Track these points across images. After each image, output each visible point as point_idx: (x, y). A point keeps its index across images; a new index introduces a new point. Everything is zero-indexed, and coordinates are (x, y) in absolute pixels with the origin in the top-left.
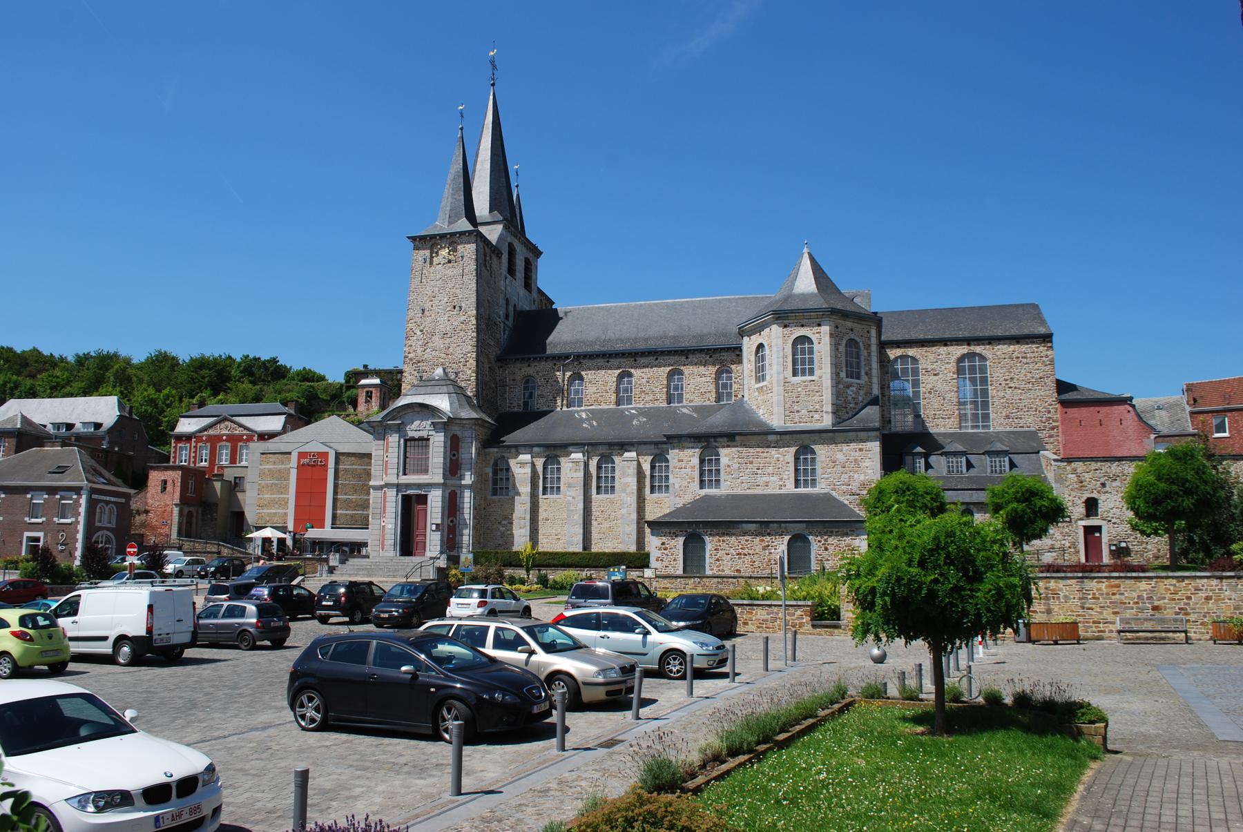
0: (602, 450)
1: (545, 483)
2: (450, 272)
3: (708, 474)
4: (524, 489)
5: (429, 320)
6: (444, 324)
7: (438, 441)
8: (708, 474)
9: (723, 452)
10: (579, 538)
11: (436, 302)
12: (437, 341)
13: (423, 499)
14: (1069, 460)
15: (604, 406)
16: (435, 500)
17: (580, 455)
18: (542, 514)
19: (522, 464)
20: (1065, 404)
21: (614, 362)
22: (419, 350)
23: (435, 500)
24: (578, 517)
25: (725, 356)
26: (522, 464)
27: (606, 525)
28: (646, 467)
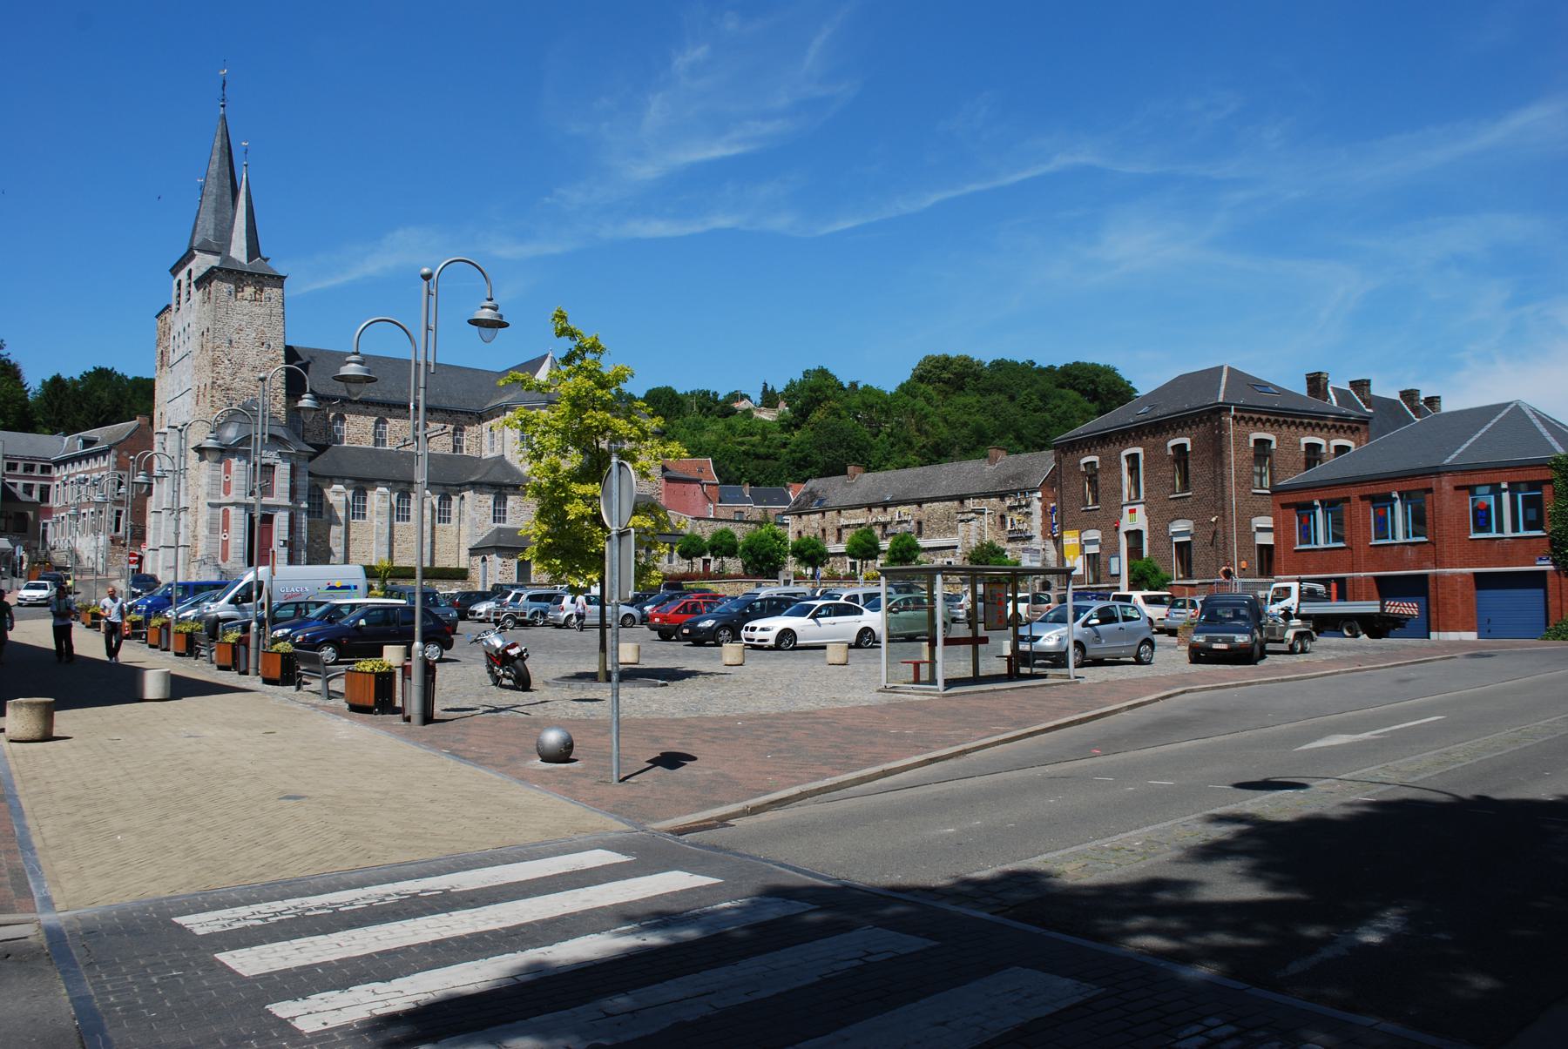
0: (401, 486)
1: (357, 509)
2: (257, 310)
3: (499, 515)
4: (341, 514)
5: (237, 351)
6: (252, 357)
7: (283, 469)
8: (499, 515)
9: (510, 498)
10: (386, 555)
11: (243, 335)
12: (245, 372)
13: (268, 519)
14: (698, 519)
15: (364, 445)
16: (281, 521)
17: (384, 490)
18: (352, 536)
19: (338, 493)
20: (669, 480)
21: (373, 409)
22: (228, 379)
23: (281, 521)
24: (385, 539)
25: (462, 418)
26: (338, 493)
27: (404, 546)
28: (436, 503)
